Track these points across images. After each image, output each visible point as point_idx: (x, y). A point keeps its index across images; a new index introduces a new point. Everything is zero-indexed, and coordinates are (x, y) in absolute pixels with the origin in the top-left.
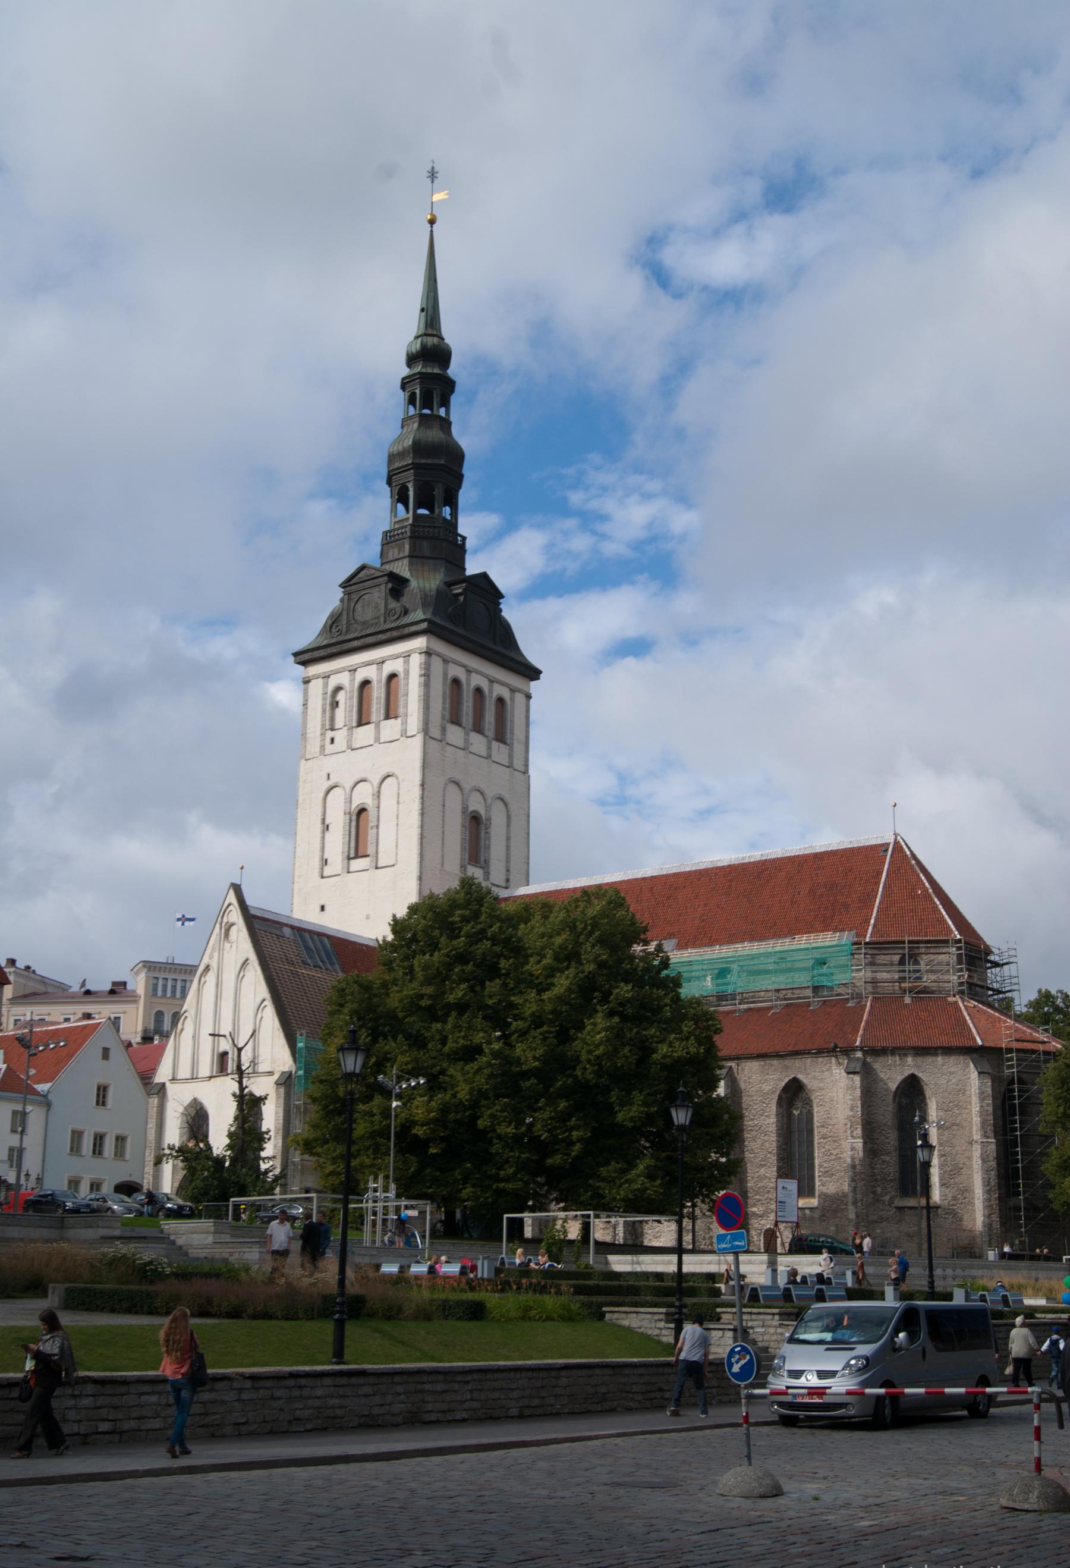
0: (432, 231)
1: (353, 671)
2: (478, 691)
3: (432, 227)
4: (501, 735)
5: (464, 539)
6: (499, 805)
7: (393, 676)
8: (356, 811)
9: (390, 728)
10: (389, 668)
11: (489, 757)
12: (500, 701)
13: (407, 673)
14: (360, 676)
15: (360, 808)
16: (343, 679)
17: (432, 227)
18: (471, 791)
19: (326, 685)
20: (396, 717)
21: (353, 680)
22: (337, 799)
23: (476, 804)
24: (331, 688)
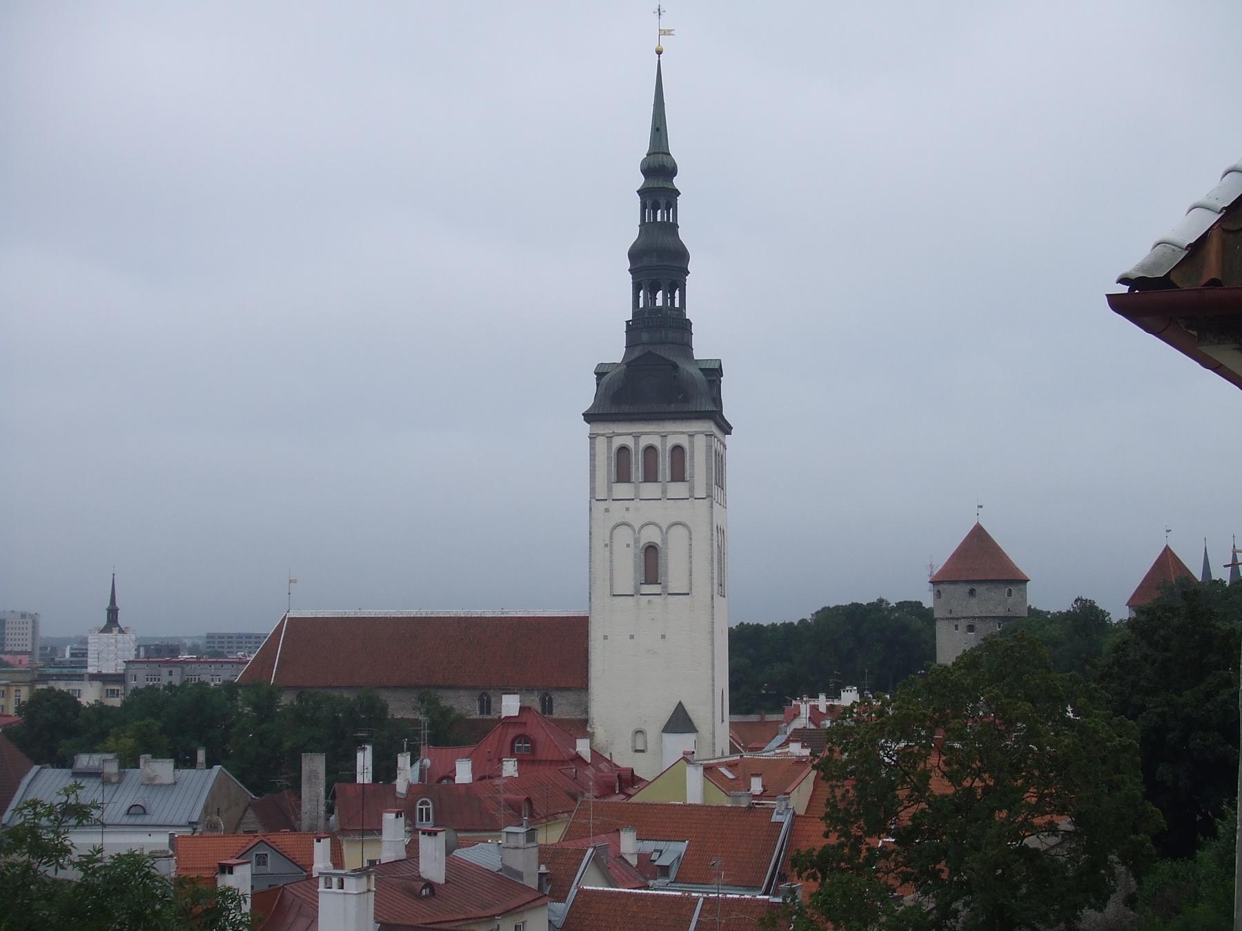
0: (659, 61)
1: (637, 437)
3: (659, 57)
7: (678, 450)
9: (678, 489)
14: (644, 441)
15: (647, 545)
16: (629, 442)
17: (659, 57)
20: (683, 480)
21: (637, 444)
22: (624, 535)
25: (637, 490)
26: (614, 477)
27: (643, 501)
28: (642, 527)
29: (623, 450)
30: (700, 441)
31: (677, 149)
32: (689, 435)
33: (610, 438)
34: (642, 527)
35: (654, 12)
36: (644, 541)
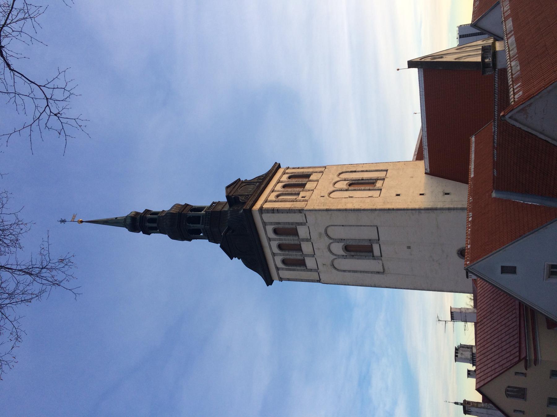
0: (85, 222)
1: (274, 254)
2: (284, 187)
4: (307, 176)
5: (213, 203)
6: (343, 176)
7: (276, 231)
8: (347, 253)
9: (302, 232)
10: (271, 235)
11: (318, 181)
12: (290, 178)
13: (271, 224)
14: (276, 250)
16: (278, 260)
18: (335, 188)
19: (283, 269)
23: (343, 185)
24: (283, 266)
25: (308, 256)
26: (302, 268)
27: (315, 253)
28: (333, 254)
29: (284, 262)
30: (267, 217)
31: (124, 212)
32: (265, 226)
33: (278, 269)
34: (333, 254)
35: (64, 223)
36: (342, 252)
